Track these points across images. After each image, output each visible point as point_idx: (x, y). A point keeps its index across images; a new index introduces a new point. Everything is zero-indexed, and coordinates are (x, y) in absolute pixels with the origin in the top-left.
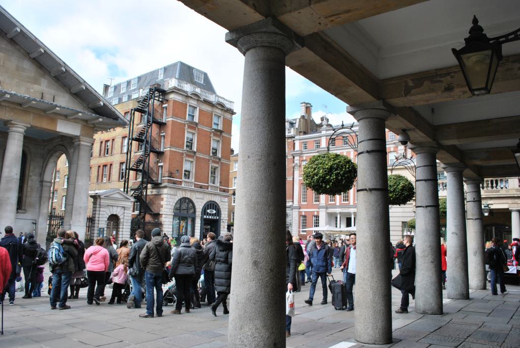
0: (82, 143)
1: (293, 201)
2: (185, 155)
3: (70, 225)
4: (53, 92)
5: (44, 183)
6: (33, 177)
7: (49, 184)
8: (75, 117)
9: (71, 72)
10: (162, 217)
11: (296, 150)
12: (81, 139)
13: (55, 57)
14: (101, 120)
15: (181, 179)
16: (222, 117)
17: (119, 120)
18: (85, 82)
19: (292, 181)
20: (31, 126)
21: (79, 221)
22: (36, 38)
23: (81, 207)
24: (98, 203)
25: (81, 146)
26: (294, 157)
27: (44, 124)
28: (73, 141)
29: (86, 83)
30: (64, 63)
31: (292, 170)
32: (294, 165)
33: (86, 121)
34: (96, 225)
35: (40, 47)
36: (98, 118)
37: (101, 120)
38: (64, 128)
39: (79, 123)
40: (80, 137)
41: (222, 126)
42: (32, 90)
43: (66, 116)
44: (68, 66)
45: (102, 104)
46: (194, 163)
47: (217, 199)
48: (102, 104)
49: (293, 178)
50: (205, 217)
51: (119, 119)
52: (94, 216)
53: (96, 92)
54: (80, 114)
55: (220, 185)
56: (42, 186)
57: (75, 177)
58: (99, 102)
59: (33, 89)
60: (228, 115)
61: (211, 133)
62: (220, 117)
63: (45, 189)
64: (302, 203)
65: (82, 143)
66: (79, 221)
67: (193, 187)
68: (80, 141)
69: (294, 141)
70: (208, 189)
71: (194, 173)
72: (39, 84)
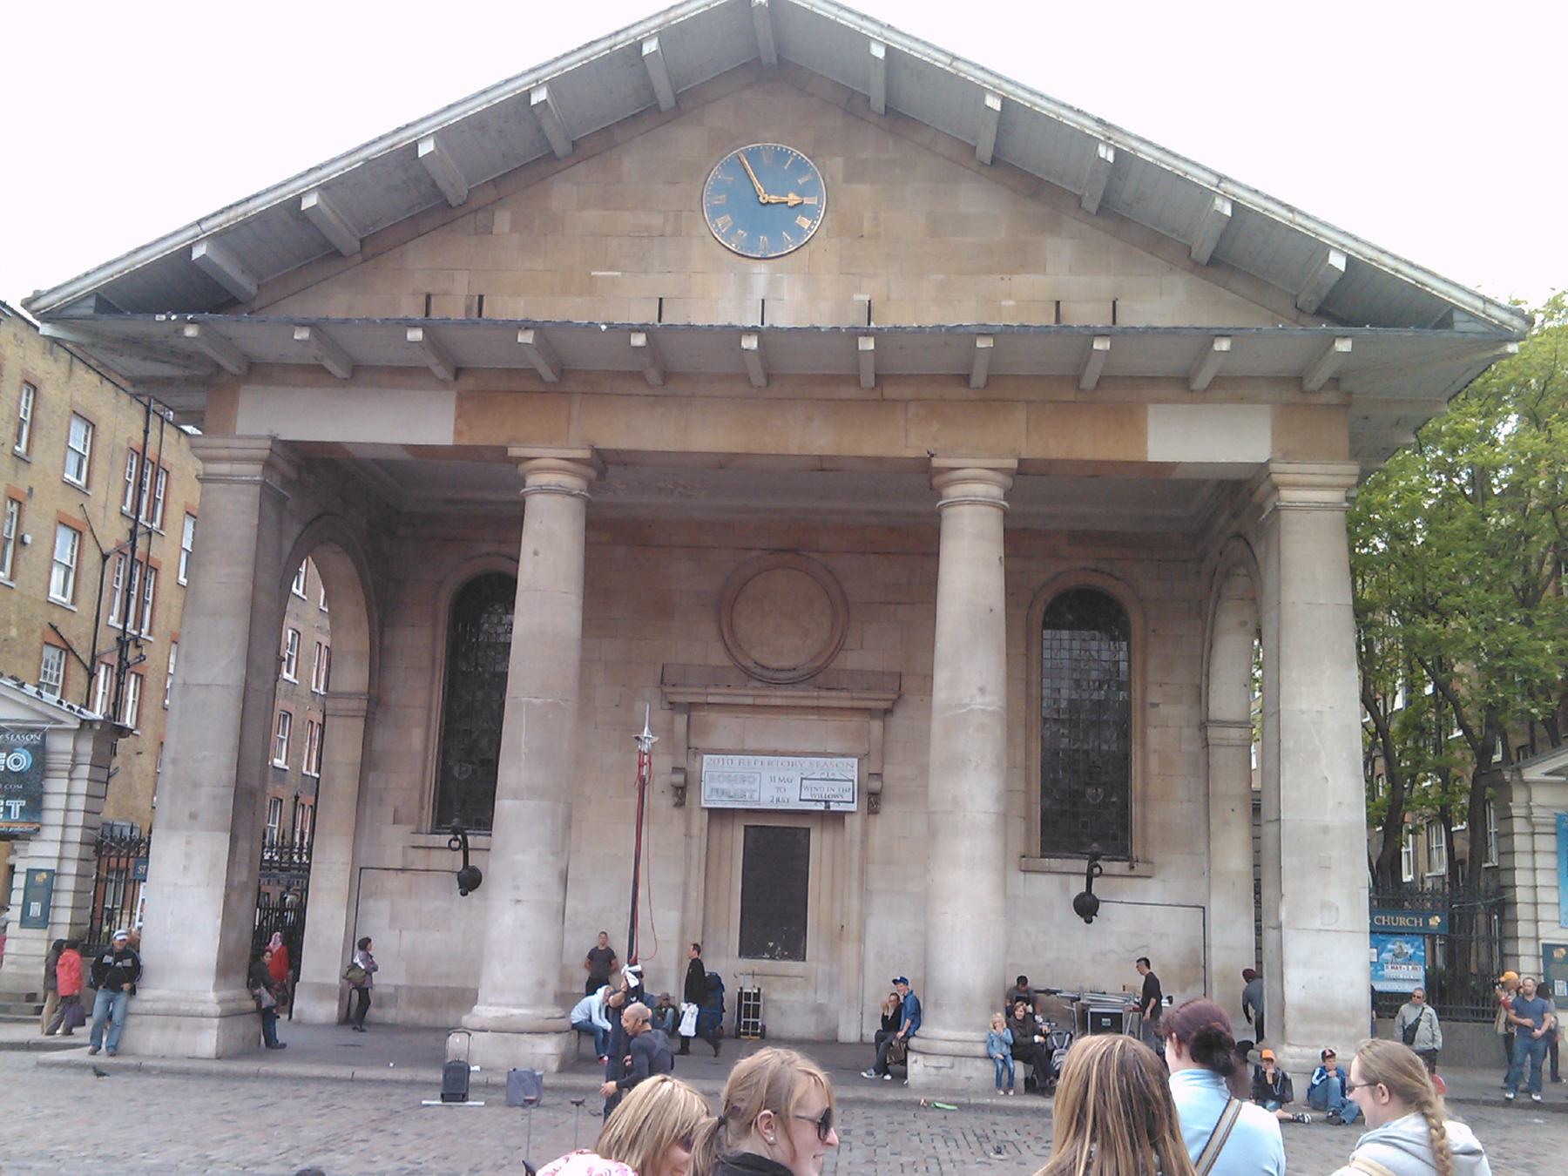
0: (1287, 495)
4: (1105, 283)
5: (1213, 733)
6: (1163, 710)
7: (1235, 734)
9: (1146, 153)
12: (1276, 478)
13: (1050, 110)
14: (1344, 346)
17: (1461, 324)
18: (1221, 178)
20: (1021, 461)
21: (1325, 906)
25: (1284, 514)
27: (1087, 444)
28: (1257, 498)
29: (1231, 181)
30: (1100, 122)
33: (1297, 381)
37: (1344, 346)
38: (1184, 440)
39: (1253, 401)
40: (1274, 467)
42: (1011, 303)
43: (1188, 379)
44: (1120, 131)
45: (1338, 262)
48: (1338, 262)
51: (1457, 316)
53: (1291, 209)
54: (1223, 345)
56: (1206, 745)
59: (1009, 297)
63: (1220, 756)
65: (1287, 495)
66: (1325, 906)
68: (1276, 488)
72: (1040, 268)
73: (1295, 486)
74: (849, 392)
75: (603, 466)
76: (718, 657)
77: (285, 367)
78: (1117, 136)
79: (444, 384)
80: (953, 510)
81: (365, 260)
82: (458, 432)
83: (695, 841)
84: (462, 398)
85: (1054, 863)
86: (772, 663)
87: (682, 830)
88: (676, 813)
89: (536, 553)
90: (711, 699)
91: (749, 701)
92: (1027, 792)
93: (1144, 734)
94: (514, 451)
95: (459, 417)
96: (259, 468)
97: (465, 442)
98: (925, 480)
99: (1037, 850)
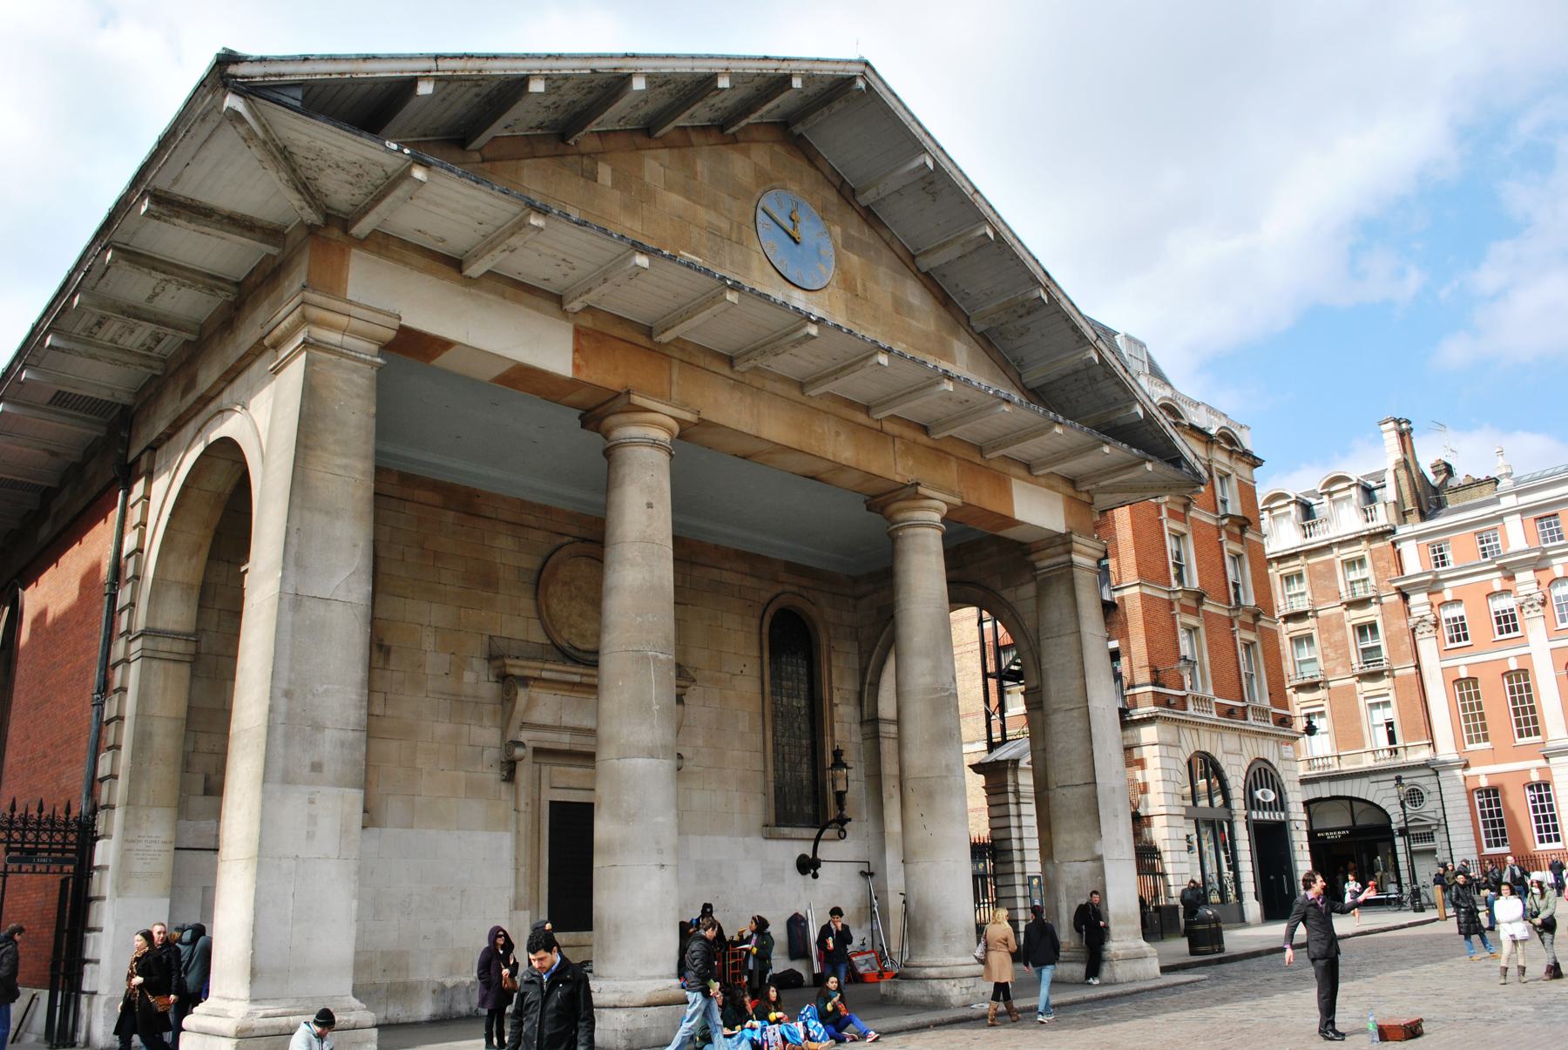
1: (1432, 744)
2: (1177, 608)
3: (1100, 859)
8: (1053, 469)
10: (1149, 825)
11: (1407, 573)
15: (1182, 689)
16: (1234, 476)
19: (1415, 680)
22: (977, 191)
23: (1113, 790)
24: (1010, 789)
26: (1405, 597)
30: (1047, 274)
31: (1407, 639)
32: (1412, 622)
34: (1017, 867)
35: (982, 219)
36: (1144, 461)
41: (1238, 504)
46: (1202, 631)
47: (1268, 750)
49: (1418, 667)
50: (1254, 815)
52: (1001, 834)
55: (1272, 703)
57: (1077, 683)
58: (1132, 407)
60: (1242, 469)
61: (1219, 529)
62: (1228, 476)
64: (1470, 747)
67: (1215, 716)
69: (1394, 544)
70: (1245, 718)
71: (1208, 669)
73: (1079, 552)
74: (861, 418)
75: (687, 434)
76: (537, 636)
77: (404, 243)
78: (1052, 287)
79: (565, 314)
80: (911, 530)
81: (483, 161)
82: (576, 367)
83: (522, 816)
84: (579, 333)
85: (786, 831)
86: (578, 644)
87: (511, 805)
88: (504, 786)
89: (650, 506)
90: (545, 675)
91: (577, 679)
92: (765, 772)
93: (832, 729)
94: (637, 399)
95: (576, 351)
96: (374, 348)
97: (583, 377)
98: (885, 501)
99: (772, 821)
